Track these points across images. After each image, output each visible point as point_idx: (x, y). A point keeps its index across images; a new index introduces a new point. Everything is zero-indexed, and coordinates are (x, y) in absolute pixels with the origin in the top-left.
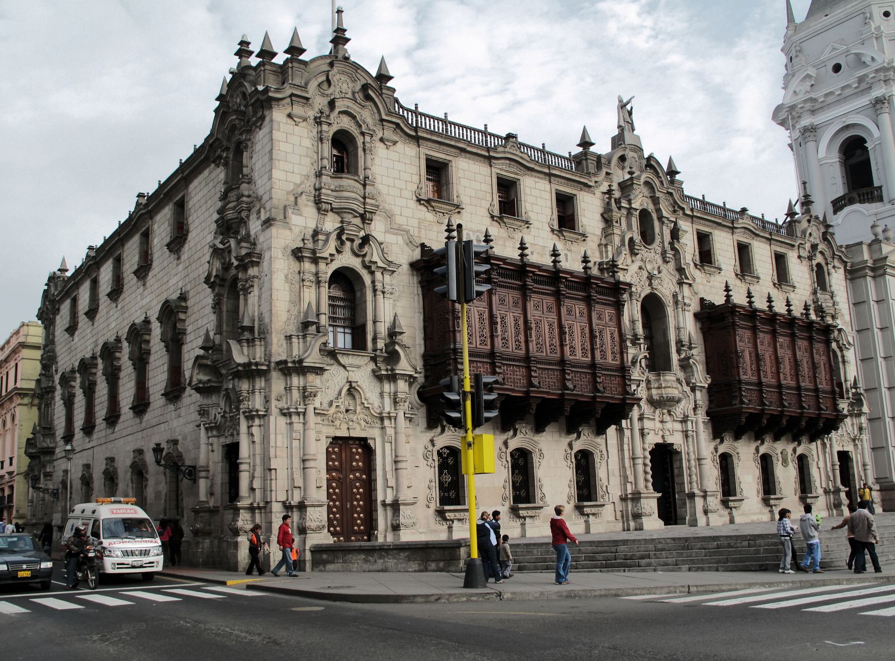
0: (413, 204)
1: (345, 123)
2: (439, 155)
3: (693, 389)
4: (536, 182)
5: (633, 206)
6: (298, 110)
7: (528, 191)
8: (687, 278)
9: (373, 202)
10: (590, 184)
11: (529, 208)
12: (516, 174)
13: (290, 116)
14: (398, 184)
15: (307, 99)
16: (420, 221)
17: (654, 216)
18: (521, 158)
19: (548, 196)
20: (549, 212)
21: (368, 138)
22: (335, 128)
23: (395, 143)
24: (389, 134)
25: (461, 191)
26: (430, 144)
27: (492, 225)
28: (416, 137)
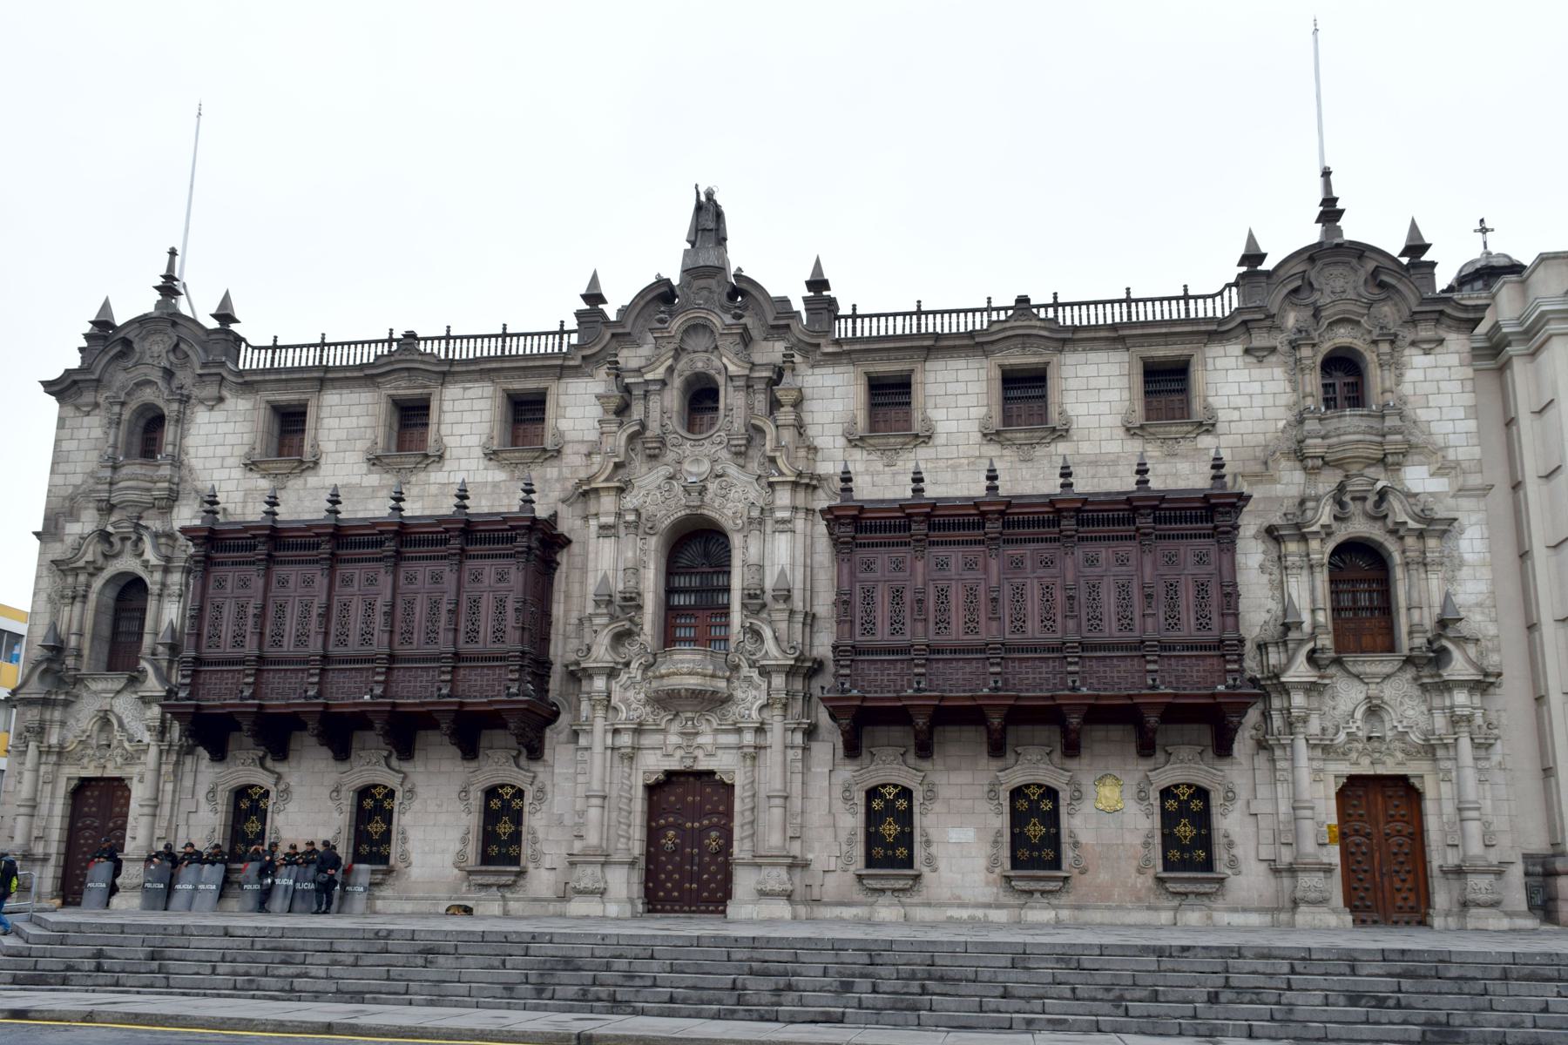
0: (237, 473)
1: (148, 395)
2: (286, 397)
3: (765, 672)
4: (465, 389)
5: (649, 376)
6: (88, 397)
7: (447, 406)
8: (781, 474)
9: (166, 485)
10: (572, 363)
11: (445, 429)
12: (425, 387)
13: (77, 408)
14: (220, 451)
15: (98, 381)
16: (247, 493)
17: (721, 380)
18: (423, 362)
19: (484, 404)
20: (485, 428)
21: (175, 406)
22: (133, 405)
23: (221, 399)
24: (211, 390)
25: (323, 435)
26: (269, 386)
27: (370, 472)
28: (249, 383)
